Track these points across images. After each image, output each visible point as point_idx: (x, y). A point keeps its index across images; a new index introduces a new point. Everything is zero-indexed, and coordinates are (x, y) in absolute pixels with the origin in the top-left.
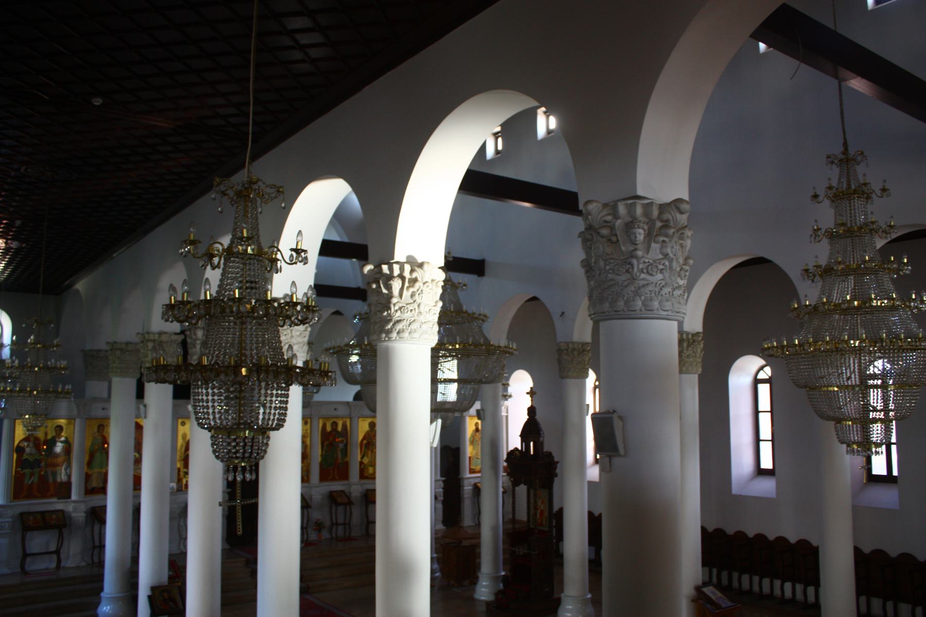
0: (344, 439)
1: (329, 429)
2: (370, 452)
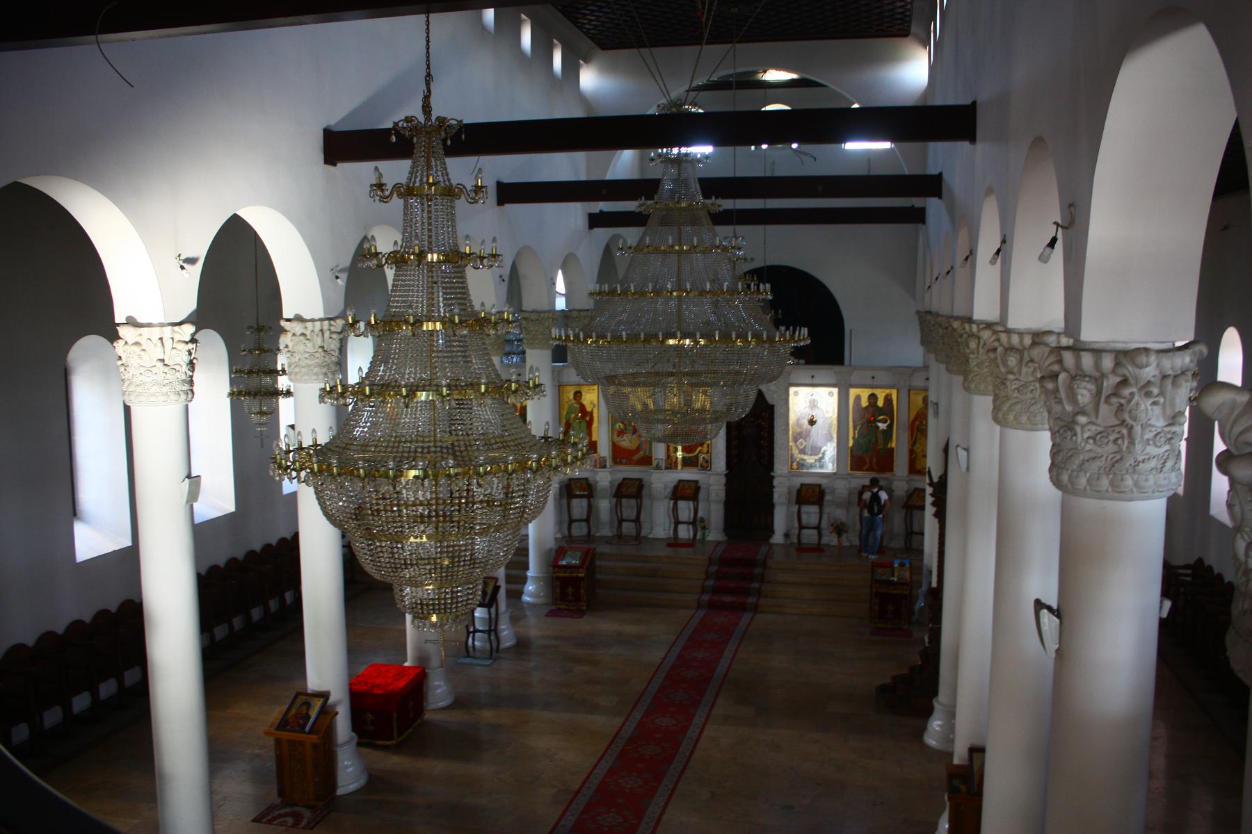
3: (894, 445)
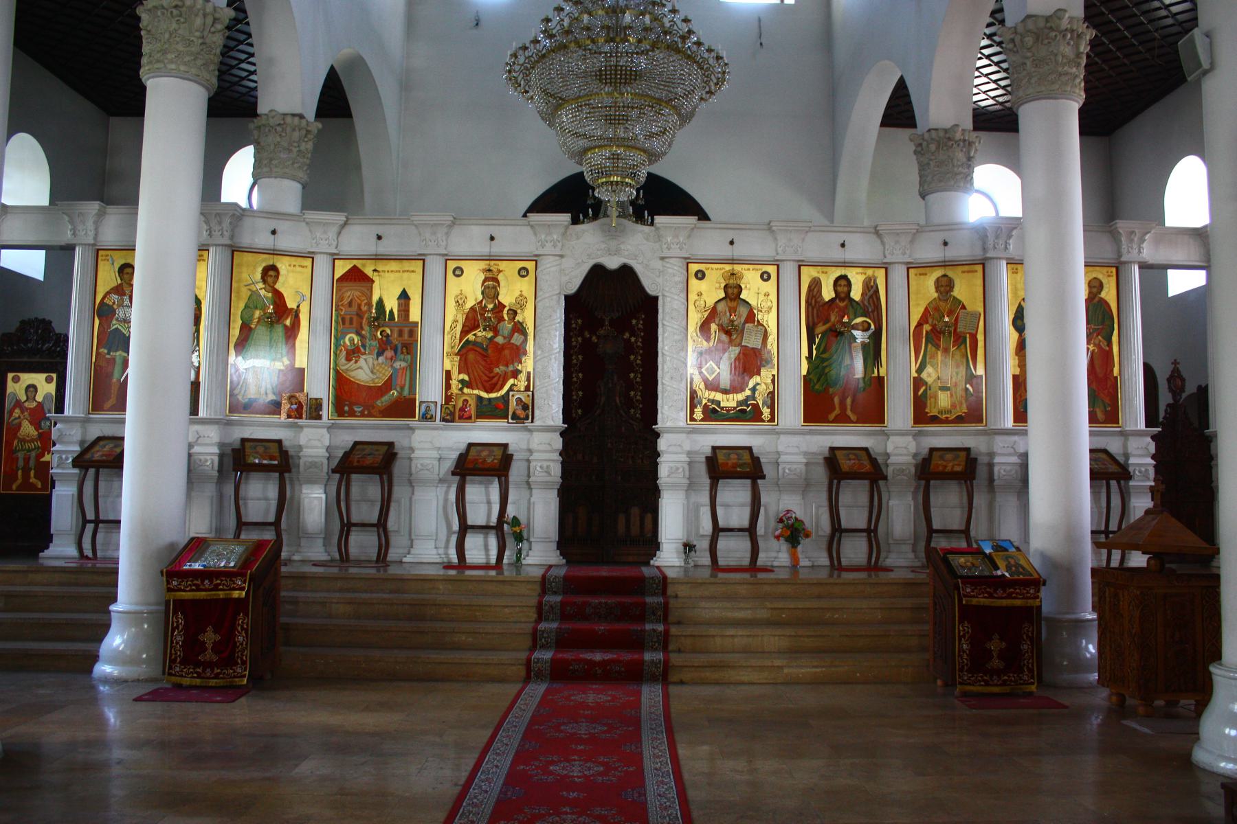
0: (868, 320)
1: (828, 293)
2: (939, 353)
3: (883, 372)
